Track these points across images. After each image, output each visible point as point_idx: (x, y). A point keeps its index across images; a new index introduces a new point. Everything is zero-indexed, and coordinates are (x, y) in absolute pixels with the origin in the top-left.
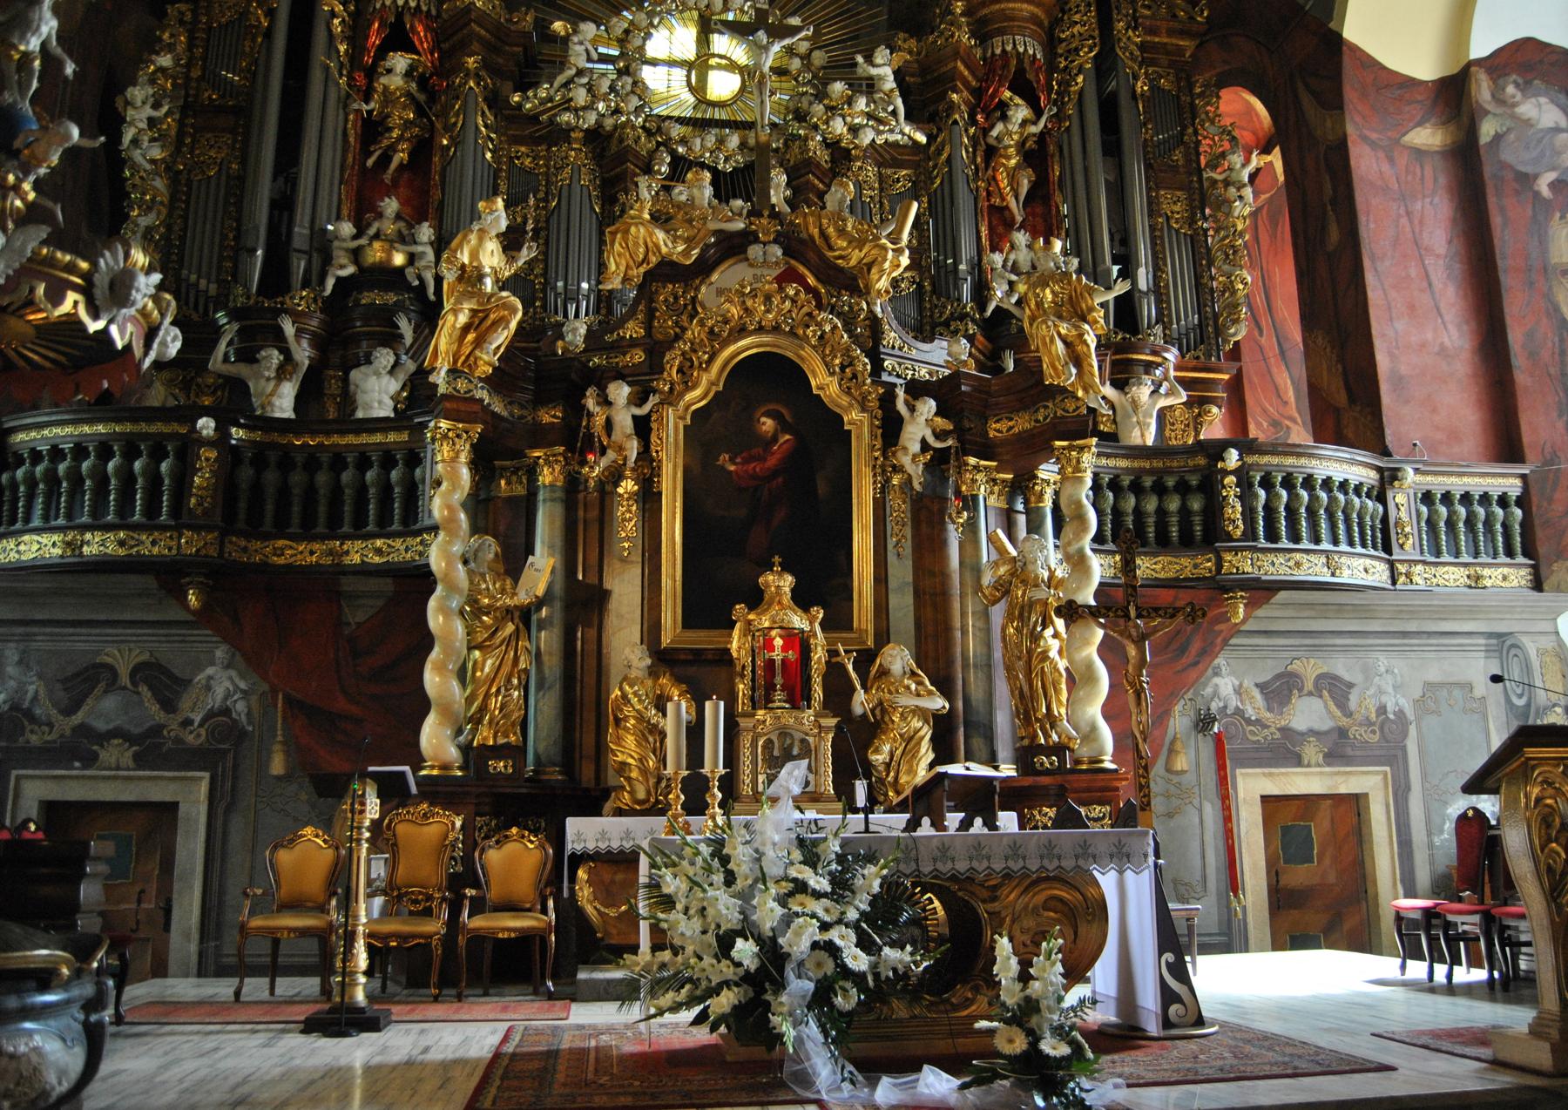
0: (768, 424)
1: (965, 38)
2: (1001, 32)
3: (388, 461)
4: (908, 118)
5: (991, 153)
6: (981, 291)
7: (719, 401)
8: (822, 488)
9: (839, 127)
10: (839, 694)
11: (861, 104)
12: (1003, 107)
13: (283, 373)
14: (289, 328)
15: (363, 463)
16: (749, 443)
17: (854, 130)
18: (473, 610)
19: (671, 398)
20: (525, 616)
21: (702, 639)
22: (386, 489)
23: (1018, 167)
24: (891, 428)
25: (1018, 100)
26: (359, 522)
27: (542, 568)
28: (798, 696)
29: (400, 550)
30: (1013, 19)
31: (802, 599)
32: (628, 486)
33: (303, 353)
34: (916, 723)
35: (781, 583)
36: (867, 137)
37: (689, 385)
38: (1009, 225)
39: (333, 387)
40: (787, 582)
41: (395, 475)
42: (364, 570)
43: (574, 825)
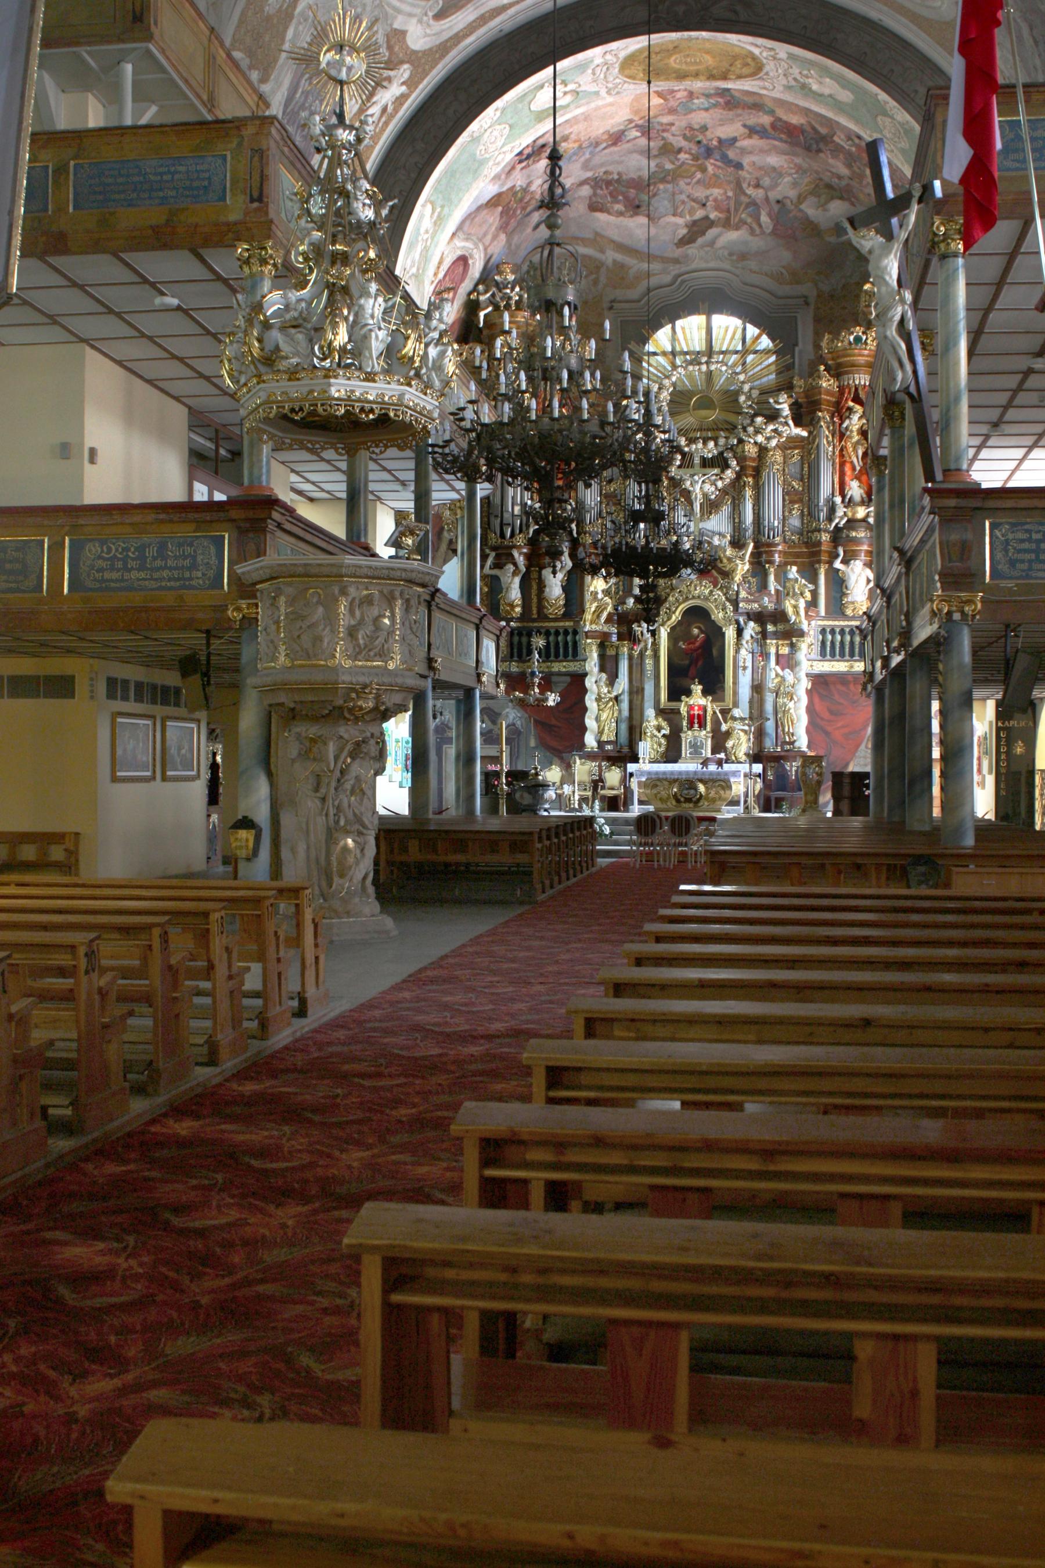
0: (696, 631)
1: (827, 383)
2: (847, 373)
3: (566, 633)
4: (797, 424)
5: (842, 436)
6: (832, 509)
7: (680, 623)
8: (715, 652)
9: (760, 439)
10: (716, 724)
11: (771, 427)
12: (850, 410)
13: (514, 574)
14: (516, 553)
15: (557, 633)
16: (690, 639)
17: (768, 439)
18: (599, 699)
19: (663, 625)
20: (616, 698)
21: (673, 705)
22: (566, 643)
23: (858, 443)
24: (740, 632)
25: (858, 407)
26: (557, 655)
27: (623, 683)
28: (702, 725)
29: (572, 667)
30: (853, 365)
31: (705, 693)
32: (648, 652)
33: (521, 560)
34: (742, 734)
35: (697, 689)
36: (774, 443)
37: (669, 619)
38: (854, 469)
39: (534, 575)
40: (700, 687)
41: (569, 638)
42: (560, 674)
43: (629, 765)
